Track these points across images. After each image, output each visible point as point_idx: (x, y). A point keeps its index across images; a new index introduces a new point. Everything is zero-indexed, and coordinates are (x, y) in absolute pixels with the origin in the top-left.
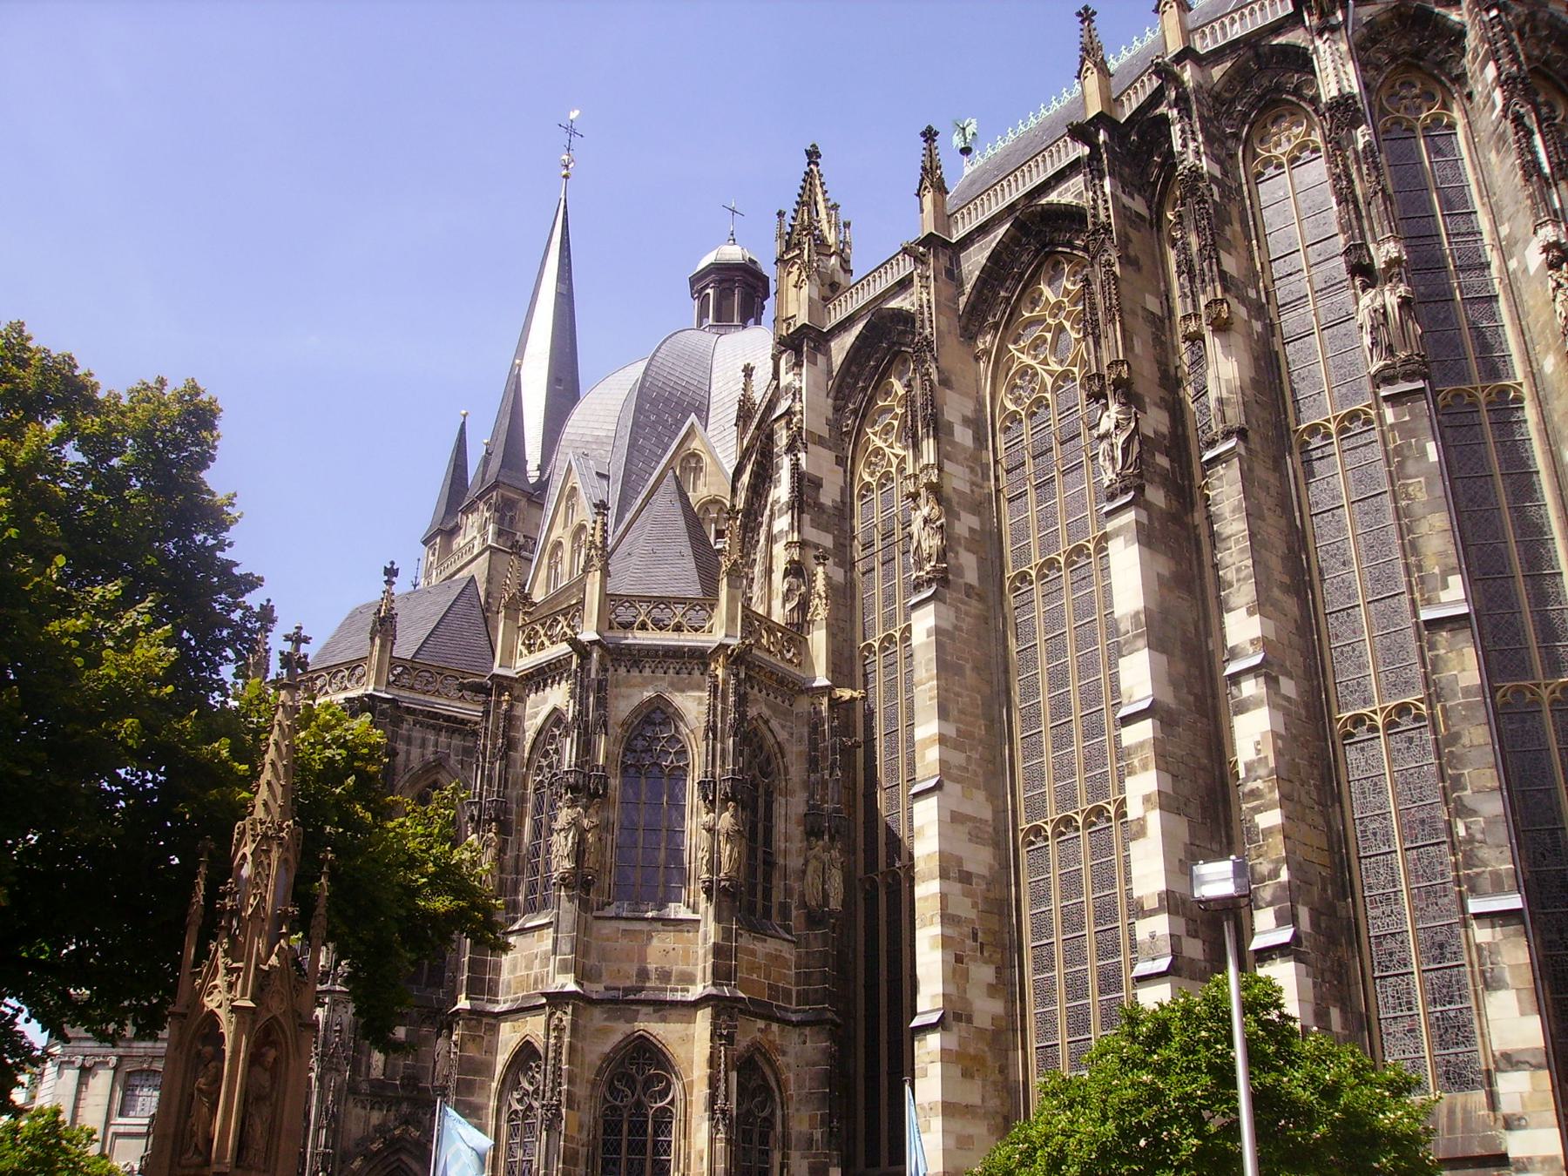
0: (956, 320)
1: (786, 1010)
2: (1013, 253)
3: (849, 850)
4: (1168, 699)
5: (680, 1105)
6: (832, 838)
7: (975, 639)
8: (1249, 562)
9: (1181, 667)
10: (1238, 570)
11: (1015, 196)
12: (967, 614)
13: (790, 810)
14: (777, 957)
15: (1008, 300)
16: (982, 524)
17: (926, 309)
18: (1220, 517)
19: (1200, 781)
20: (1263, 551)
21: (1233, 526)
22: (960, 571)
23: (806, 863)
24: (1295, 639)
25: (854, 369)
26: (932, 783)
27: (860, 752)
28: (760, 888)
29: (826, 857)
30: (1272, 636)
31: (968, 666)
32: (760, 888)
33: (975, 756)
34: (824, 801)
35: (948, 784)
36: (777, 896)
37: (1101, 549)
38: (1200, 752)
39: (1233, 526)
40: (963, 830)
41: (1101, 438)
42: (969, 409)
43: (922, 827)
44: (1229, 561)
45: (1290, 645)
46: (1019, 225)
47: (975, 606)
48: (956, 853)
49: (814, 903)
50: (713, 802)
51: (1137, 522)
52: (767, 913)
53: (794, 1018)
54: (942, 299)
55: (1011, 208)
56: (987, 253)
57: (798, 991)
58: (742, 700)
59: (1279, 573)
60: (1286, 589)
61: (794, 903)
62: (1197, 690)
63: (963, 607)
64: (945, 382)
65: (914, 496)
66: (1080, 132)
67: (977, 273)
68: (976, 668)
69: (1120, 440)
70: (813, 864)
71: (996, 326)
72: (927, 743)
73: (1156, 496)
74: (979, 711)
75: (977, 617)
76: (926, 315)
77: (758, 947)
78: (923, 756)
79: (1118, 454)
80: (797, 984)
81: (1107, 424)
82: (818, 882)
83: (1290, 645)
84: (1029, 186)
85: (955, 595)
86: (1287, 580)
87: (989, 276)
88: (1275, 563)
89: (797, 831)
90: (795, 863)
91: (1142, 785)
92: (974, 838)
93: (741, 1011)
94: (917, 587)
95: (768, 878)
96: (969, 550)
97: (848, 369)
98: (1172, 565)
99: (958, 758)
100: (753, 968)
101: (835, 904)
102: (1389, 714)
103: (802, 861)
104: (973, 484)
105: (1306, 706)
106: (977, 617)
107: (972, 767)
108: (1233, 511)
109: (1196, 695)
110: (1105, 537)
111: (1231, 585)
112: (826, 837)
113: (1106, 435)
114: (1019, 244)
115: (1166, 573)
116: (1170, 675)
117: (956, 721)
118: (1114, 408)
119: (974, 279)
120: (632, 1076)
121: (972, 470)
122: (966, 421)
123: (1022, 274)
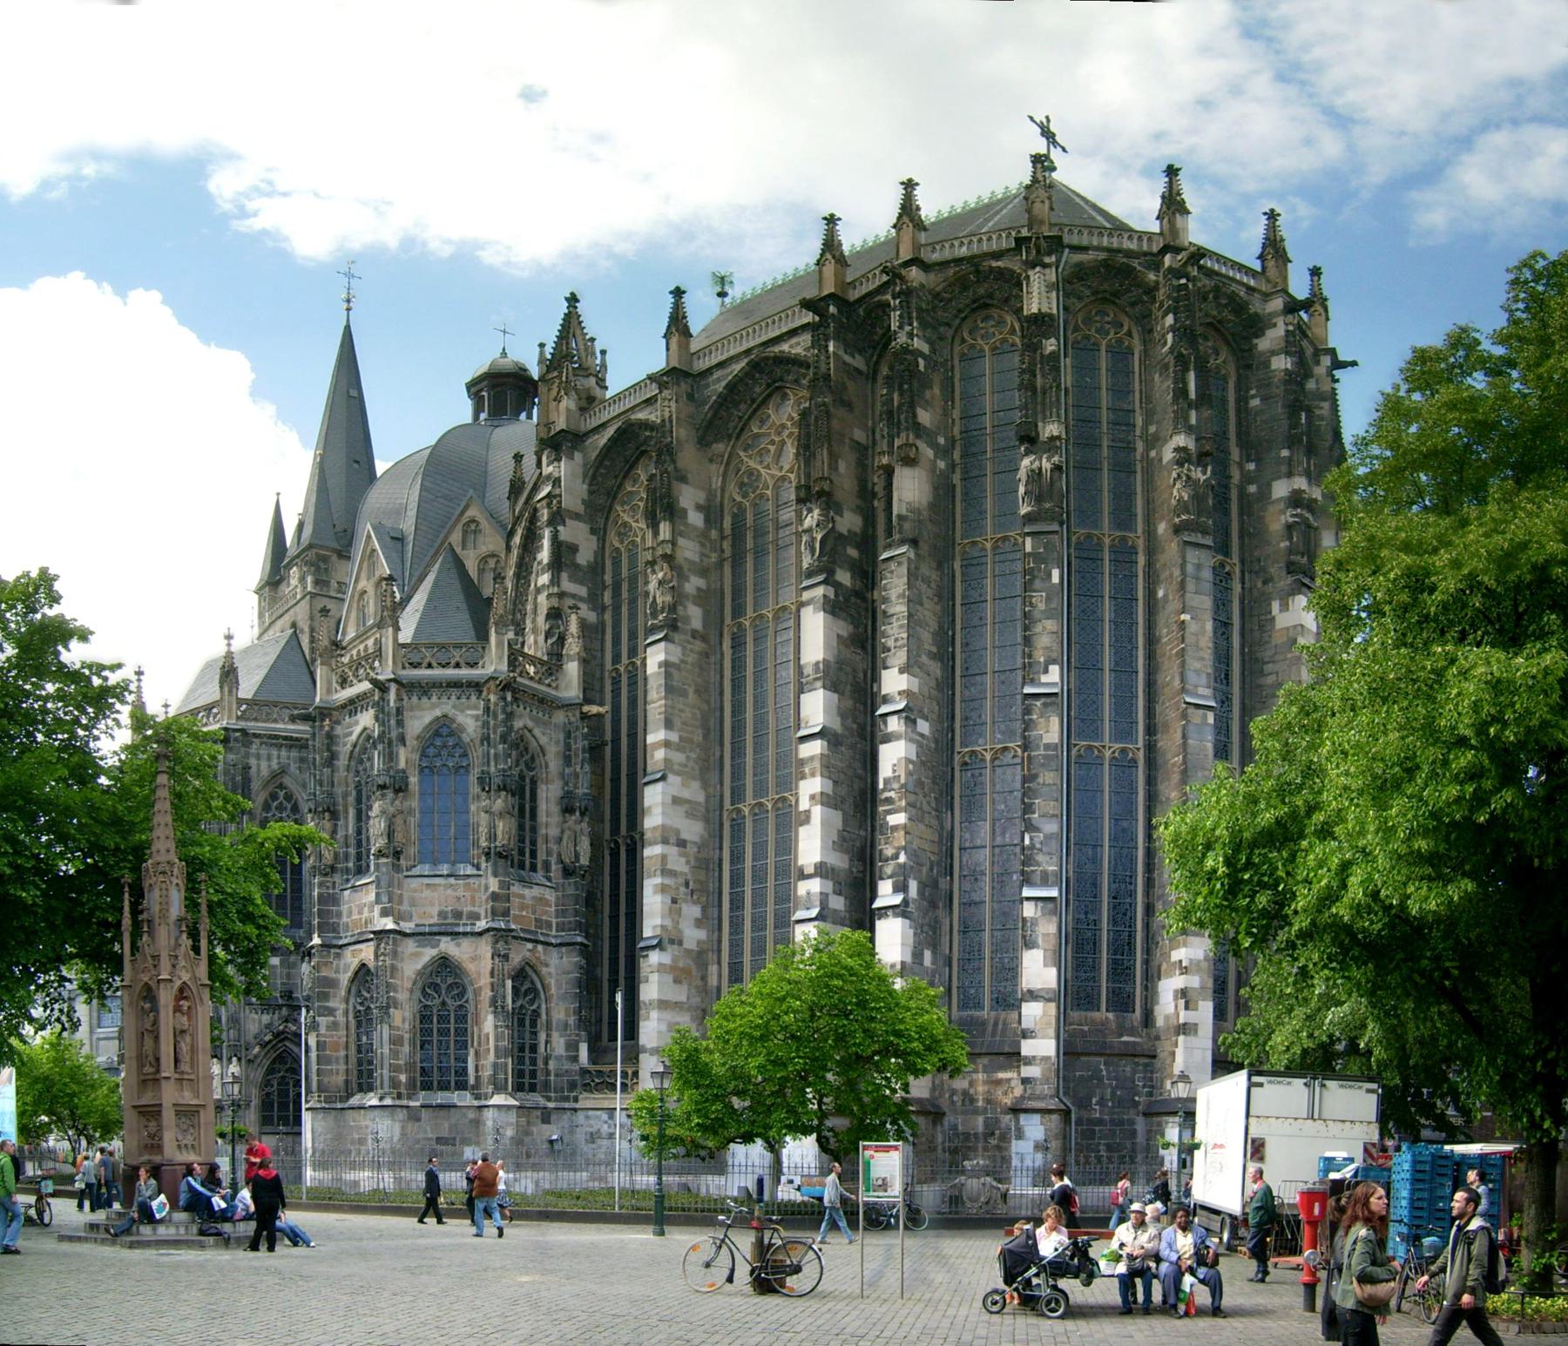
2: (747, 384)
3: (597, 819)
4: (836, 725)
5: (472, 1002)
6: (582, 814)
7: (697, 670)
8: (905, 635)
9: (849, 703)
10: (896, 640)
11: (752, 344)
12: (692, 651)
14: (541, 899)
16: (708, 583)
18: (886, 600)
19: (856, 787)
20: (918, 628)
21: (898, 608)
22: (687, 619)
23: (562, 832)
24: (934, 693)
26: (659, 776)
27: (608, 749)
28: (527, 850)
29: (578, 828)
30: (916, 690)
31: (691, 691)
32: (527, 850)
33: (693, 755)
34: (576, 787)
35: (671, 778)
36: (541, 856)
37: (798, 611)
38: (857, 765)
39: (898, 608)
40: (681, 810)
41: (805, 531)
42: (701, 497)
43: (650, 807)
44: (890, 632)
45: (930, 697)
46: (755, 366)
47: (699, 645)
48: (678, 826)
51: (825, 596)
52: (533, 868)
55: (748, 352)
56: (724, 384)
59: (928, 644)
60: (932, 656)
61: (553, 860)
62: (861, 720)
63: (689, 646)
66: (807, 305)
68: (697, 691)
69: (819, 537)
70: (567, 833)
71: (730, 436)
72: (657, 745)
73: (844, 577)
74: (698, 723)
75: (700, 653)
77: (527, 892)
78: (652, 756)
79: (818, 545)
81: (809, 521)
82: (571, 845)
83: (930, 697)
84: (764, 338)
85: (682, 637)
86: (934, 649)
87: (726, 400)
88: (927, 637)
89: (555, 809)
90: (553, 832)
91: (810, 787)
92: (690, 815)
93: (514, 937)
95: (533, 843)
96: (695, 604)
98: (851, 628)
99: (678, 757)
100: (522, 908)
101: (584, 860)
102: (996, 753)
103: (559, 830)
104: (702, 555)
105: (936, 741)
106: (700, 653)
107: (691, 763)
108: (898, 597)
109: (858, 724)
110: (802, 605)
111: (889, 650)
112: (578, 813)
113: (809, 530)
114: (753, 378)
115: (845, 634)
116: (839, 708)
117: (679, 731)
118: (816, 512)
121: (702, 545)
122: (699, 508)
123: (753, 401)
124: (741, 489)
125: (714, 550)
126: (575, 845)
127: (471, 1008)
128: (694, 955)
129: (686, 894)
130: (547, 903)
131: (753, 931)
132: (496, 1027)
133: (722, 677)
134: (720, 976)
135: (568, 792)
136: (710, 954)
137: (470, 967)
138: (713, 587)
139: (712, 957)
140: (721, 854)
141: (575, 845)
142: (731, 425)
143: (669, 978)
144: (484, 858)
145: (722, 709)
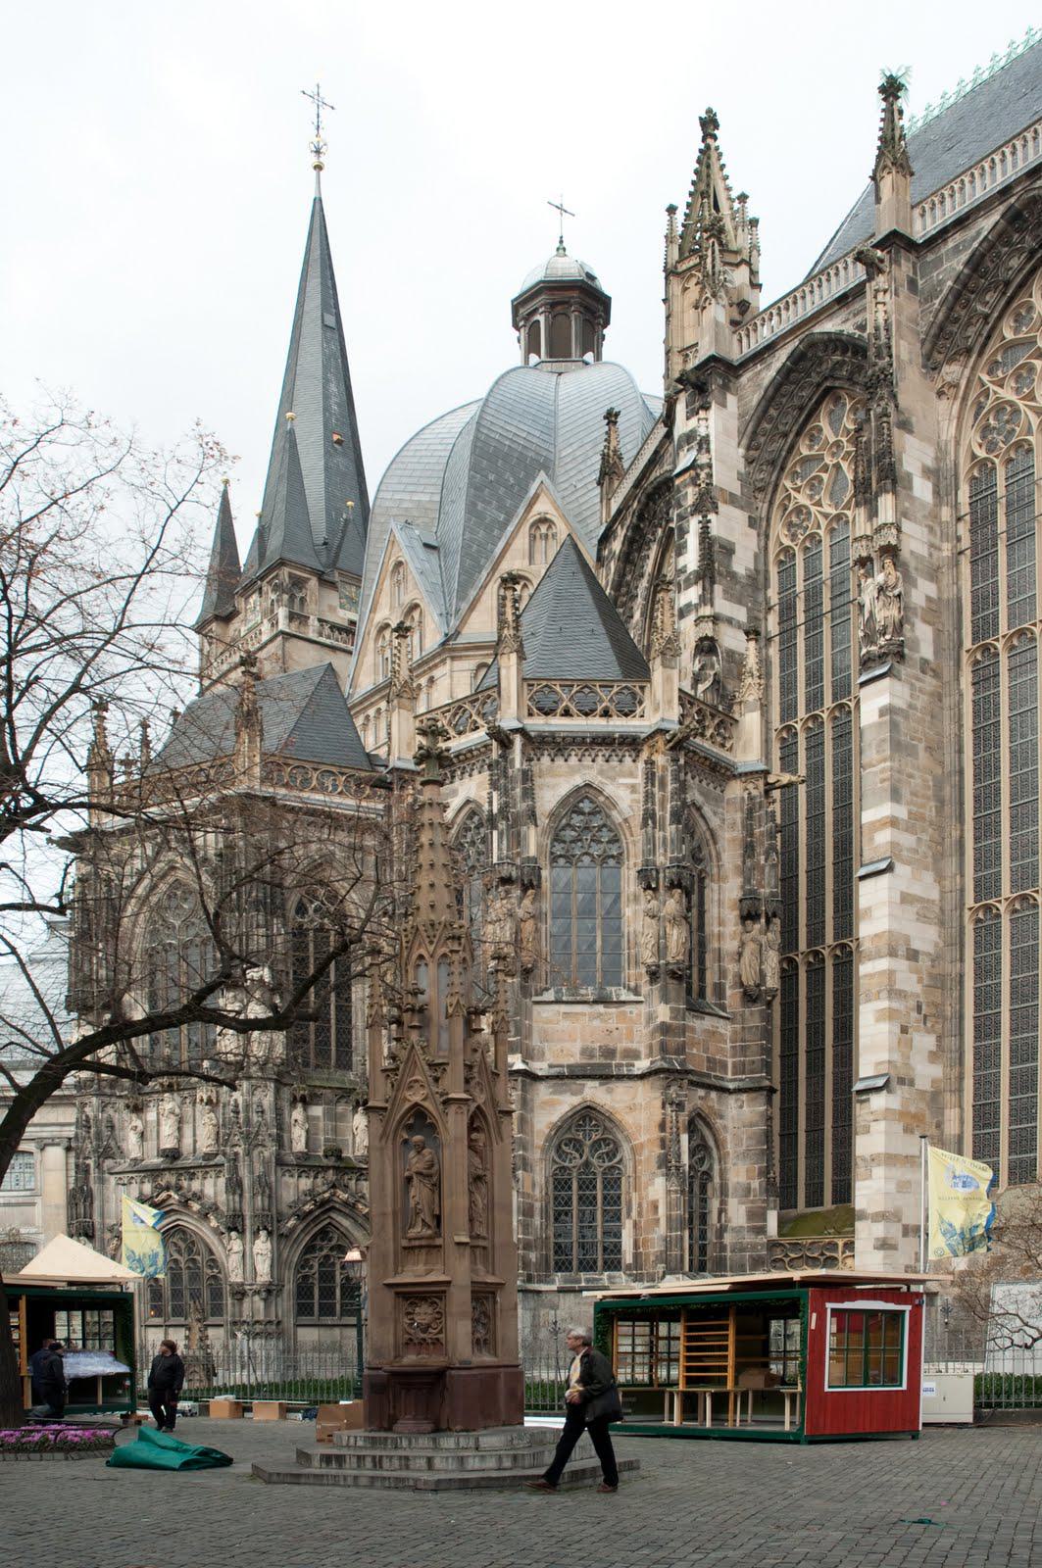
0: (919, 345)
1: (722, 1079)
13: (725, 894)
15: (986, 317)
17: (883, 333)
25: (772, 412)
49: (752, 983)
50: (655, 890)
53: (731, 1086)
54: (903, 319)
57: (734, 1063)
58: (682, 788)
64: (905, 426)
65: (864, 562)
67: (950, 283)
71: (969, 351)
76: (883, 339)
80: (734, 1056)
87: (965, 286)
94: (866, 663)
97: (765, 411)
119: (945, 292)
120: (579, 1141)
124: (983, 437)
125: (945, 537)
126: (761, 963)
127: (628, 1168)
128: (928, 1097)
129: (918, 1021)
130: (722, 1038)
131: (1012, 1064)
132: (668, 1192)
133: (961, 726)
134: (962, 1122)
135: (752, 892)
136: (947, 1096)
137: (628, 1119)
138: (945, 596)
139: (949, 1098)
140: (962, 968)
141: (761, 963)
142: (971, 331)
143: (899, 1127)
144: (647, 978)
145: (961, 772)
